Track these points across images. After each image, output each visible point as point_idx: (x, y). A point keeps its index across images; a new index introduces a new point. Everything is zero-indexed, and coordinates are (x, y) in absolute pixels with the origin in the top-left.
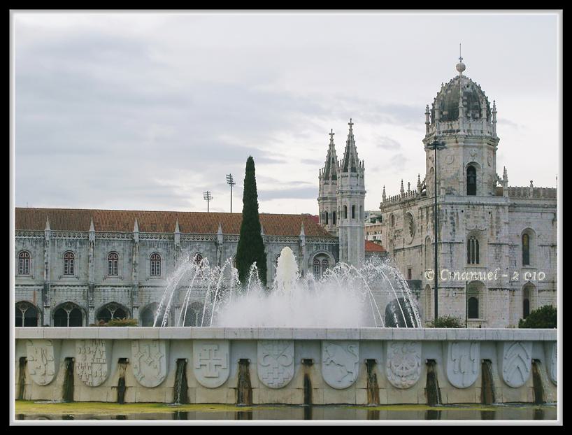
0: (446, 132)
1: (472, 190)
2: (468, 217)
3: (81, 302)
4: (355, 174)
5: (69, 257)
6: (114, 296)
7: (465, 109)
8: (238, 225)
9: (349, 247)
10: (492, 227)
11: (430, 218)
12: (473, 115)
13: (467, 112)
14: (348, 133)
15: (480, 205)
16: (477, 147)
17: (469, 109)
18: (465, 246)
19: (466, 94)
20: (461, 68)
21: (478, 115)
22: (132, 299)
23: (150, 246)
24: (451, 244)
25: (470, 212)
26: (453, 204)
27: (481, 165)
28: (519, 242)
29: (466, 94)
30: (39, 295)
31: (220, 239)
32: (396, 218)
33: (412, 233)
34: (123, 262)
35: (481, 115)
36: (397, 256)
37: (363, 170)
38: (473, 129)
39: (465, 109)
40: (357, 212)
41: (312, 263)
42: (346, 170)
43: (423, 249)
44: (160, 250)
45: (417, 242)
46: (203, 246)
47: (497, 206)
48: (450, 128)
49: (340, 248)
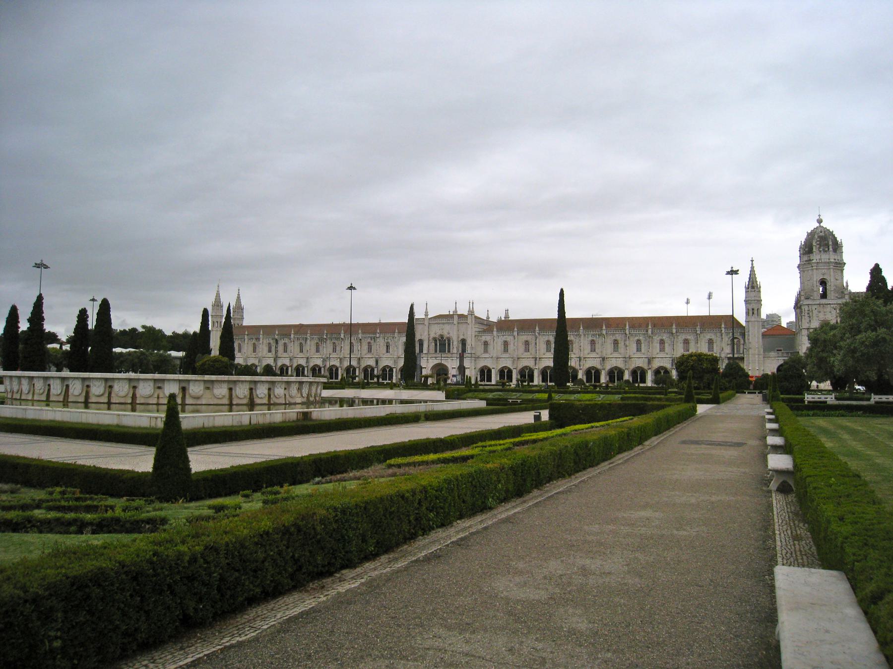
0: (806, 261)
3: (599, 367)
4: (753, 290)
5: (593, 343)
6: (616, 363)
7: (818, 246)
8: (555, 325)
9: (750, 333)
12: (823, 250)
13: (819, 248)
14: (751, 266)
15: (827, 304)
16: (826, 269)
17: (820, 246)
20: (820, 221)
21: (827, 249)
22: (626, 365)
25: (821, 310)
26: (809, 305)
29: (819, 237)
30: (578, 363)
31: (674, 331)
34: (621, 345)
37: (760, 287)
39: (818, 246)
40: (756, 312)
44: (641, 338)
46: (665, 335)
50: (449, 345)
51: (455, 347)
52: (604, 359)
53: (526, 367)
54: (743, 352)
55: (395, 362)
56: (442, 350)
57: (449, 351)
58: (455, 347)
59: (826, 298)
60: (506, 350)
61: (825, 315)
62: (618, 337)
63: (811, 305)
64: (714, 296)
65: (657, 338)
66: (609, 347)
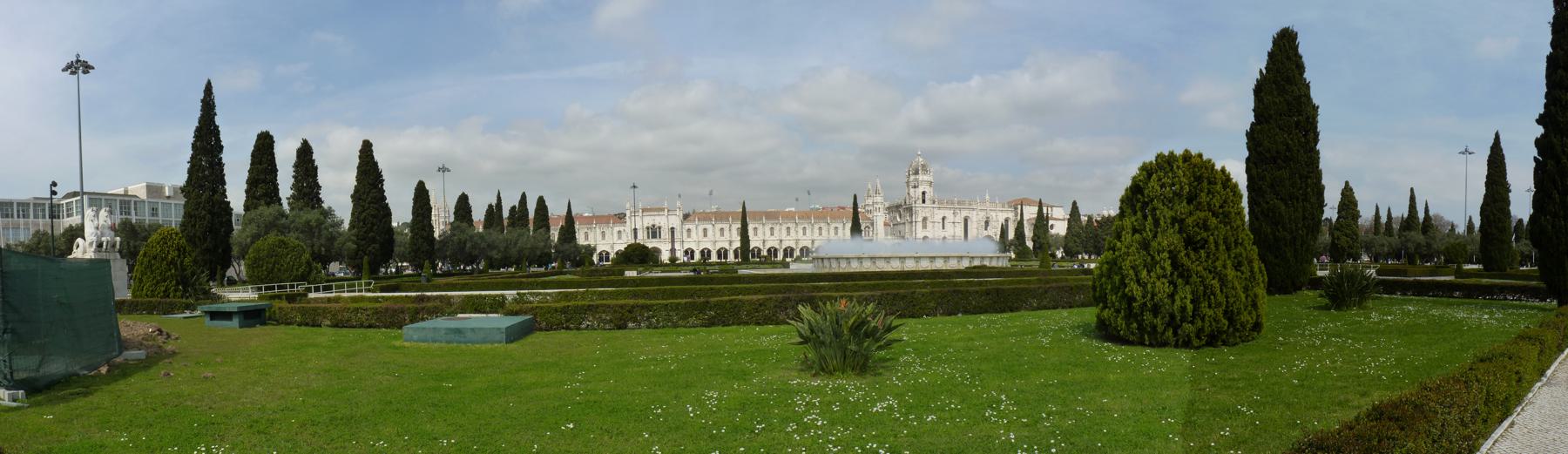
1: (924, 201)
3: (777, 247)
28: (941, 221)
34: (792, 231)
44: (806, 226)
50: (660, 232)
51: (665, 234)
52: (781, 241)
53: (722, 248)
55: (731, 243)
56: (654, 236)
57: (660, 237)
58: (665, 234)
60: (705, 235)
62: (822, 225)
64: (714, 193)
65: (817, 226)
66: (784, 232)
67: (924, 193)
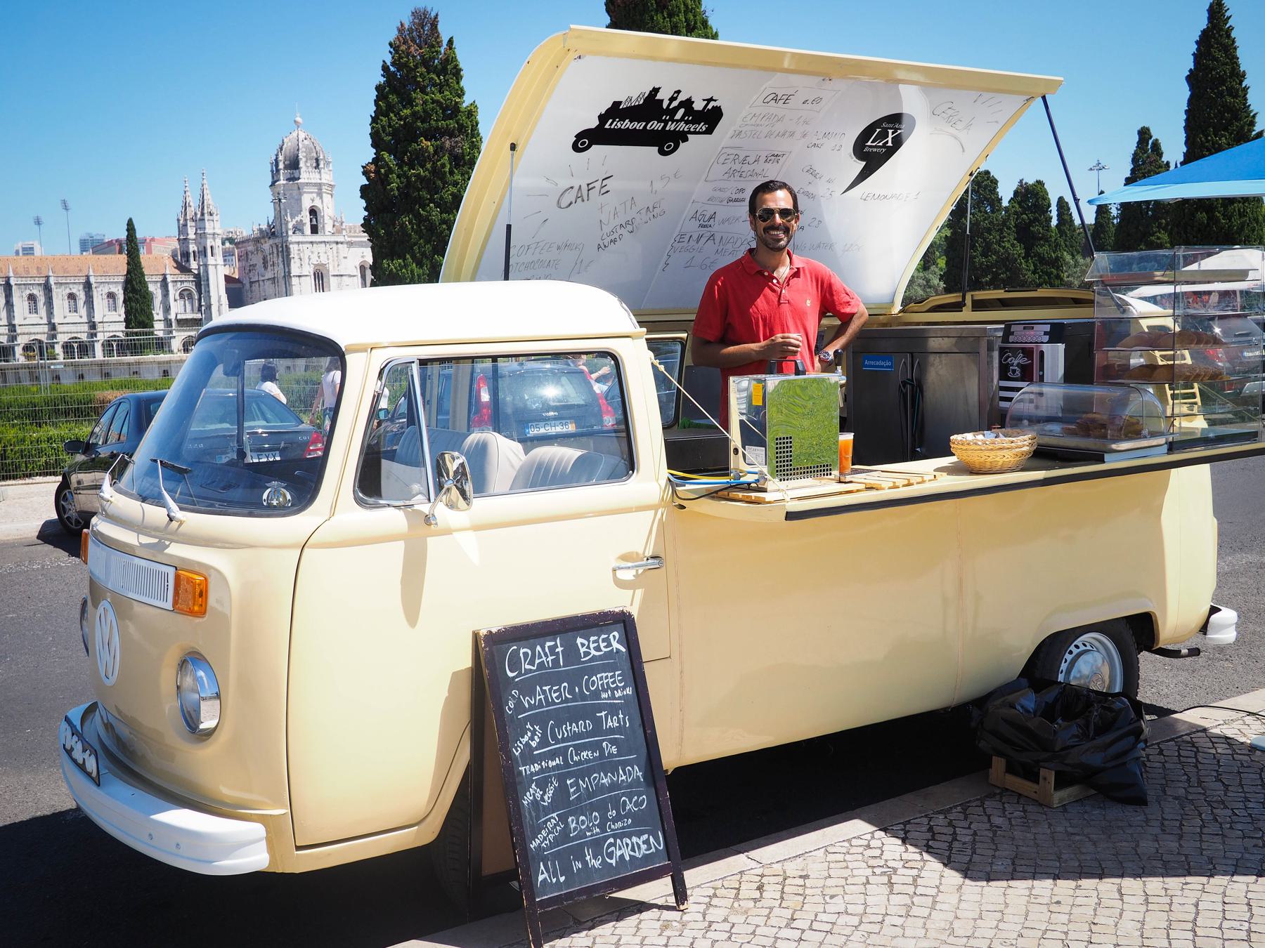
1: (314, 230)
2: (312, 252)
4: (211, 218)
10: (333, 261)
11: (280, 254)
12: (311, 165)
13: (306, 162)
15: (321, 242)
17: (307, 159)
18: (313, 277)
19: (306, 147)
23: (26, 289)
24: (299, 276)
27: (321, 209)
32: (250, 254)
33: (266, 268)
35: (318, 165)
36: (253, 288)
38: (311, 177)
40: (215, 251)
41: (178, 297)
42: (203, 214)
43: (276, 281)
45: (269, 275)
47: (337, 243)
48: (292, 176)
49: (202, 283)
54: (200, 310)
59: (317, 233)
61: (319, 257)
63: (302, 243)
67: (313, 212)
